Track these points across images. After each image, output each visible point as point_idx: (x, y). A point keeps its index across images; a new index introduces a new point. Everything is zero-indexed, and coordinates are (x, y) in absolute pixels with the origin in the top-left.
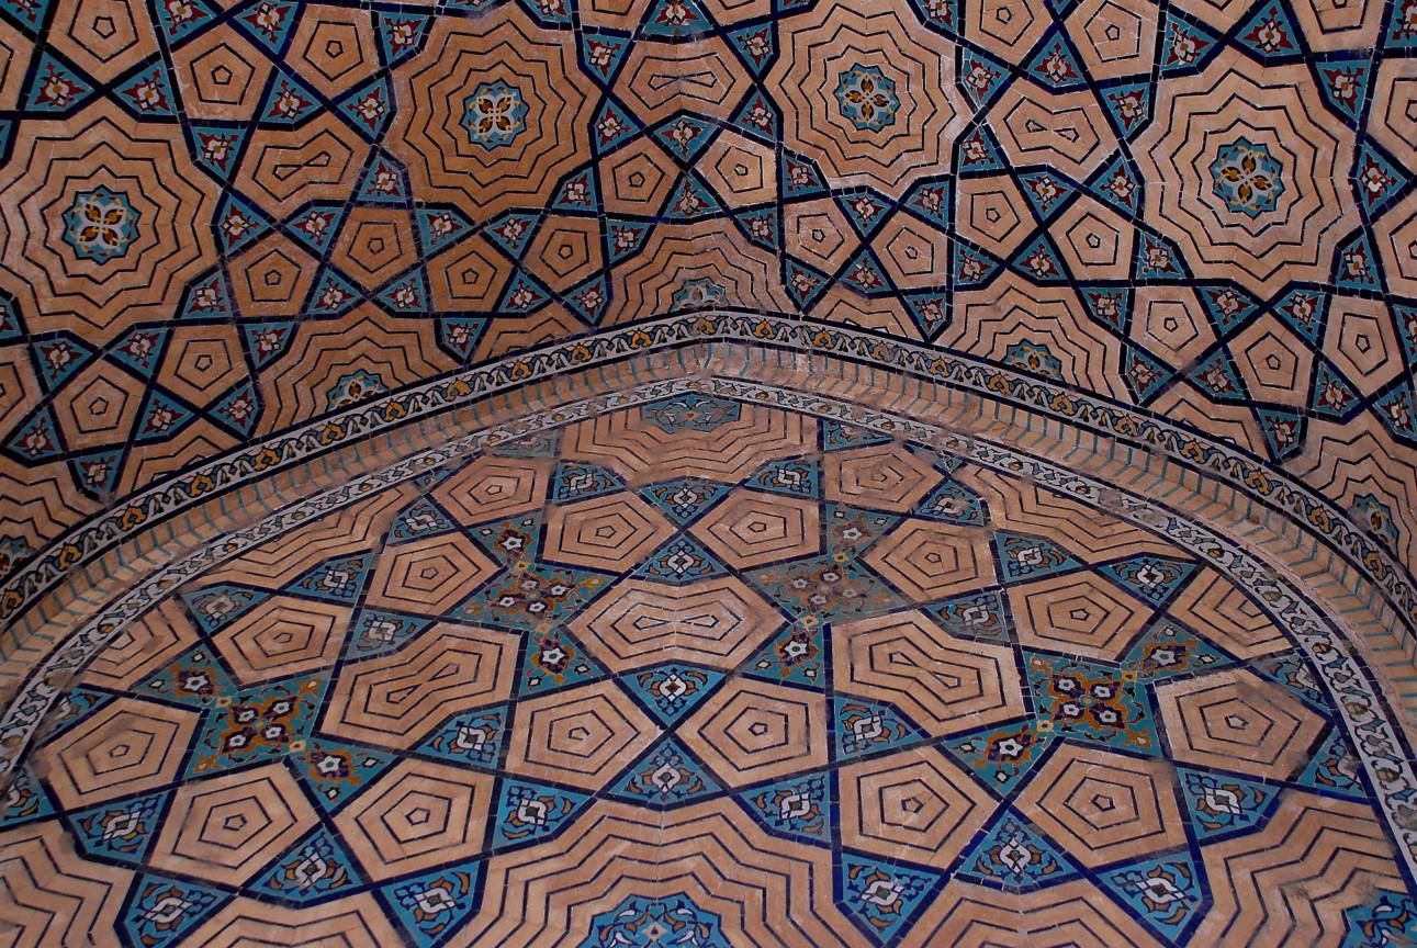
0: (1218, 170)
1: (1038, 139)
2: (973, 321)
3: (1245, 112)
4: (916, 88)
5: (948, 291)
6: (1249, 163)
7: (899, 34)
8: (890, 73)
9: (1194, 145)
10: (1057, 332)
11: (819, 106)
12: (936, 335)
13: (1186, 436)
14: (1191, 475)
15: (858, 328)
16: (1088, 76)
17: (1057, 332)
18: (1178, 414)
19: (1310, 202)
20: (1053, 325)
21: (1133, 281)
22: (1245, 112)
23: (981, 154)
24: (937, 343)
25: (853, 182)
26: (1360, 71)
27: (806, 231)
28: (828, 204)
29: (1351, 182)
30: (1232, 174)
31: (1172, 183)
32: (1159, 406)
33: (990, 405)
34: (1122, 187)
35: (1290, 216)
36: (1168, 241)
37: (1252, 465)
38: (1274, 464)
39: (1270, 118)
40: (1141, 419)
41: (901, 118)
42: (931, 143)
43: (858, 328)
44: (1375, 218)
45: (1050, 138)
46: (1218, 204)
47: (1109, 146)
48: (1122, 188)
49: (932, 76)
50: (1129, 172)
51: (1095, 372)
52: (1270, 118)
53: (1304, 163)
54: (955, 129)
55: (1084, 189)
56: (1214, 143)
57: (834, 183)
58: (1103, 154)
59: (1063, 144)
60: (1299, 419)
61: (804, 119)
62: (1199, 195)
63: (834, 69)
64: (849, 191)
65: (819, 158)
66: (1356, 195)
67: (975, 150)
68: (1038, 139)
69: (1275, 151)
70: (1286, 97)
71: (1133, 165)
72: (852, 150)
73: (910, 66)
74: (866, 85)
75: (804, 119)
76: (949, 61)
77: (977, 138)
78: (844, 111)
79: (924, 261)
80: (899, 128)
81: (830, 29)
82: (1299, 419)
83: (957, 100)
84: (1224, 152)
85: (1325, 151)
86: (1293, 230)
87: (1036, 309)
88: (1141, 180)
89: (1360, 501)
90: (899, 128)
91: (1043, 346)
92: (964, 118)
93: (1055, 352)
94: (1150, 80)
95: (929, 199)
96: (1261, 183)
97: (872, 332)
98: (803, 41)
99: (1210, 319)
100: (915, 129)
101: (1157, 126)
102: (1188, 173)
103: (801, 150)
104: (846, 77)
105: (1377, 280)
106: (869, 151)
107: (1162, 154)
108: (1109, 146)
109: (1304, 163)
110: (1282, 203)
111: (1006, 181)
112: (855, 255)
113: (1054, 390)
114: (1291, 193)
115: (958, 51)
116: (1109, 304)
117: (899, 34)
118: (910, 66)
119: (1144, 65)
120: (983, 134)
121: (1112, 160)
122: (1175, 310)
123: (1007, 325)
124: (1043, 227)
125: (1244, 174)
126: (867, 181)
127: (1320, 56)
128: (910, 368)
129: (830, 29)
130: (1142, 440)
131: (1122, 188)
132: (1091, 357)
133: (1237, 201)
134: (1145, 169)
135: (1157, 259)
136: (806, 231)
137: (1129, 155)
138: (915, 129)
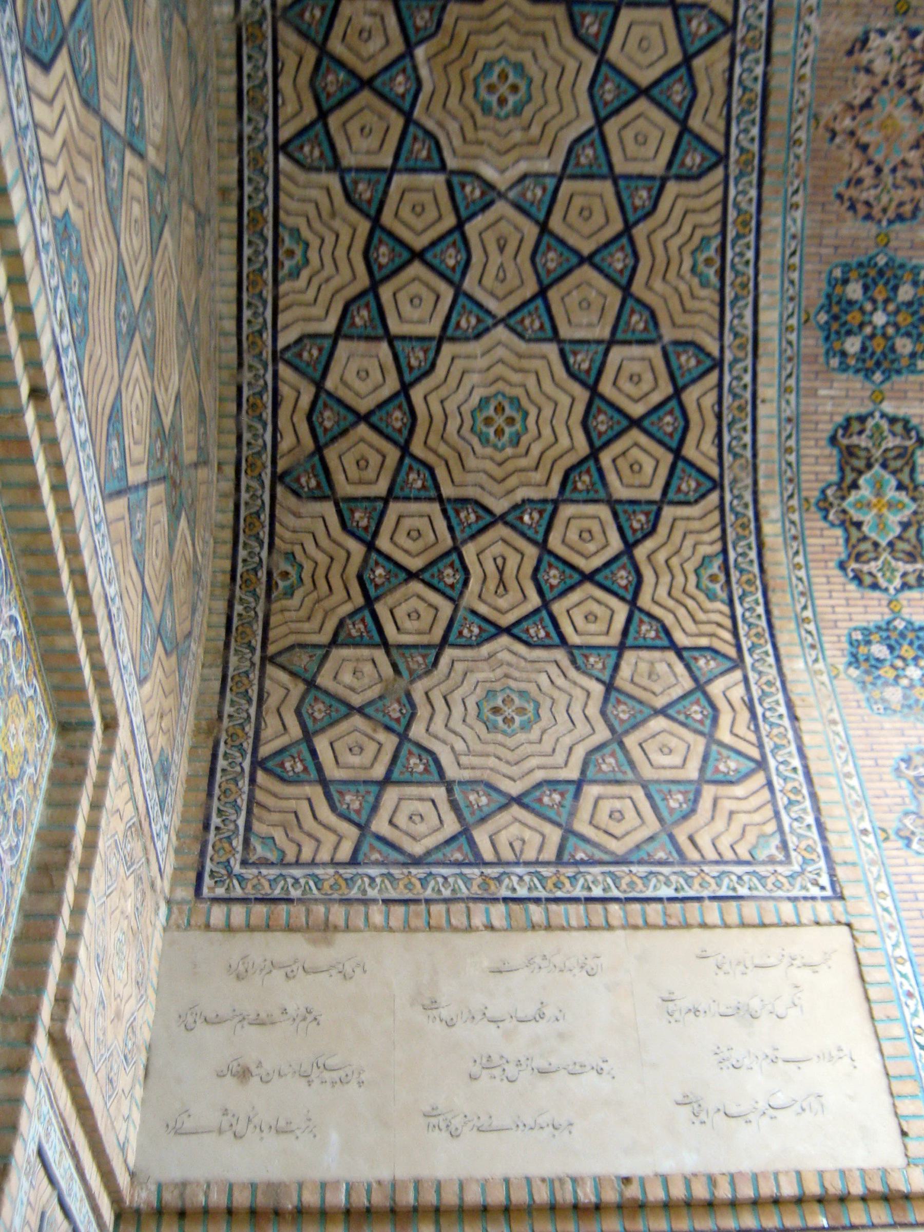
0: (500, 398)
1: (492, 248)
2: (315, 194)
3: (547, 412)
4: (517, 136)
5: (336, 166)
6: (511, 421)
7: (562, 120)
8: (528, 111)
9: (516, 378)
10: (325, 274)
11: (493, 40)
12: (290, 157)
13: (268, 398)
14: (233, 407)
15: (276, 75)
16: (551, 285)
17: (325, 274)
18: (284, 389)
19: (499, 472)
20: (329, 269)
21: (392, 340)
22: (547, 412)
23: (469, 197)
24: (282, 160)
25: (424, 72)
26: (596, 492)
27: (367, 21)
28: (398, 47)
29: (523, 501)
30: (500, 409)
31: (482, 363)
32: (284, 371)
33: (233, 212)
34: (465, 320)
35: (481, 460)
36: (433, 366)
37: (267, 457)
38: (277, 478)
39: (547, 432)
40: (267, 354)
41: (489, 121)
42: (474, 149)
43: (276, 75)
44: (506, 523)
45: (495, 258)
46: (475, 400)
47: (499, 309)
48: (468, 322)
49: (530, 150)
50: (481, 327)
51: (297, 312)
52: (547, 432)
53: (523, 462)
54: (489, 173)
55: (459, 291)
56: (519, 392)
57: (420, 53)
58: (491, 304)
59: (492, 270)
60: (325, 490)
61: (476, 25)
62: (476, 388)
63: (525, 57)
64: (415, 68)
65: (441, 39)
66: (516, 507)
67: (473, 191)
68: (492, 248)
69: (525, 440)
70: (564, 442)
71: (487, 330)
72: (454, 72)
73: (535, 131)
74: (514, 89)
75: (476, 25)
76: (545, 166)
77: (483, 194)
78: (488, 66)
79: (361, 144)
80: (481, 119)
81: (561, 55)
82: (325, 490)
83: (514, 173)
84: (515, 401)
85: (538, 477)
86: (471, 462)
87: (341, 253)
88: (478, 336)
89: (291, 557)
90: (481, 119)
91: (307, 262)
92: (501, 181)
93: (305, 274)
94: (555, 336)
95: (418, 147)
96: (499, 432)
97: (276, 91)
98: (548, 27)
99: (380, 406)
100: (482, 135)
101: (522, 346)
102: (491, 375)
103: (448, 21)
104: (520, 68)
105: (465, 535)
106: (456, 88)
107: (500, 352)
108: (499, 309)
109: (523, 462)
110: (489, 451)
111: (450, 221)
112: (352, 73)
113: (268, 274)
114: (499, 457)
115: (552, 175)
116: (364, 317)
117: (562, 120)
118: (535, 131)
119: (565, 332)
120: (487, 199)
121: (488, 312)
122: (376, 375)
123: (317, 225)
124: (418, 255)
125: (502, 416)
126: (427, 88)
127: (597, 461)
128: (248, 130)
129: (561, 55)
130: (247, 358)
131: (468, 322)
132: (310, 308)
133: (480, 417)
134: (486, 340)
135: (417, 358)
136: (367, 21)
137: (495, 325)
138: (482, 135)
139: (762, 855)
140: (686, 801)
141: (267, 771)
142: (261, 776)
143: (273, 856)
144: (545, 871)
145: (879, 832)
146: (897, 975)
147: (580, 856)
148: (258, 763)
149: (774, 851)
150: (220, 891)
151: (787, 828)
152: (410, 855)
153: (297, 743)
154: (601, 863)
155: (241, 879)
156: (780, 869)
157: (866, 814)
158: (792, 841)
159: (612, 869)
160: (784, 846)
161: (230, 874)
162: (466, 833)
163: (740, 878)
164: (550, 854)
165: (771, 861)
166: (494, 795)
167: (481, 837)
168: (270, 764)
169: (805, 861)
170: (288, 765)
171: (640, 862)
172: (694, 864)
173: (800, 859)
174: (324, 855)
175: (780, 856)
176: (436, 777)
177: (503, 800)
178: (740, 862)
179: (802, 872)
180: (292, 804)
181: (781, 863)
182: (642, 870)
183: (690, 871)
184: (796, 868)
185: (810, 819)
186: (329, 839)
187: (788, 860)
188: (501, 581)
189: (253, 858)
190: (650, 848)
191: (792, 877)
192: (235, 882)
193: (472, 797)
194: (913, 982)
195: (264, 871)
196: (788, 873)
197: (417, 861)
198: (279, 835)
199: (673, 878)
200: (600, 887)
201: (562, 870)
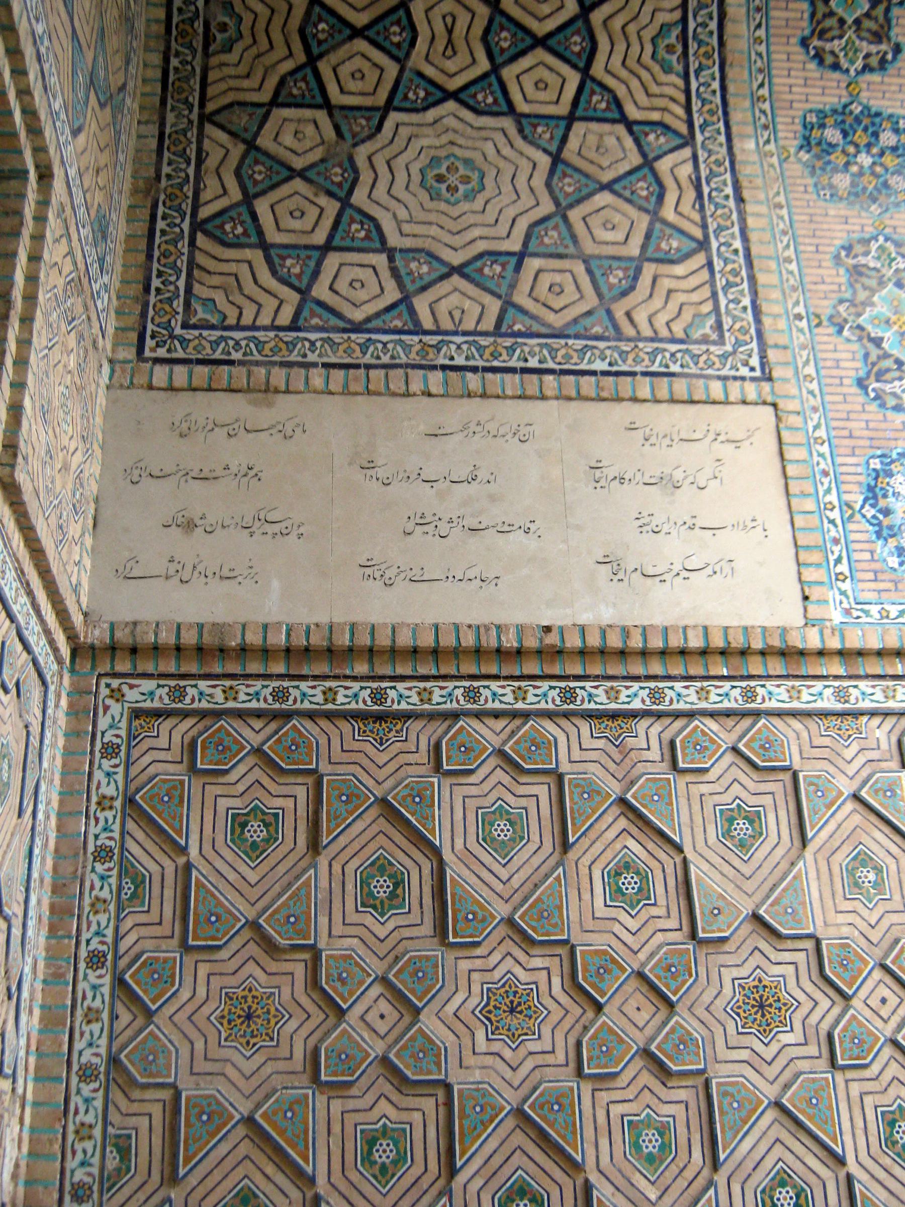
139: (697, 335)
141: (206, 233)
142: (201, 239)
143: (214, 320)
144: (484, 341)
145: (845, 508)
146: (825, 521)
147: (516, 327)
148: (197, 226)
149: (707, 330)
150: (162, 352)
151: (723, 310)
152: (350, 321)
153: (237, 205)
154: (539, 335)
155: (183, 341)
156: (712, 348)
157: (844, 554)
158: (727, 322)
159: (549, 341)
160: (719, 326)
161: (172, 337)
162: (406, 300)
163: (673, 355)
164: (488, 324)
165: (705, 340)
166: (435, 264)
167: (421, 305)
168: (209, 226)
169: (738, 343)
170: (228, 227)
171: (577, 336)
172: (629, 340)
175: (714, 337)
176: (378, 245)
177: (445, 270)
178: (674, 340)
179: (734, 352)
180: (232, 267)
181: (714, 343)
182: (579, 344)
184: (728, 348)
185: (746, 301)
186: (270, 304)
187: (721, 341)
188: (450, 41)
189: (193, 321)
190: (587, 322)
191: (724, 357)
194: (840, 528)
195: (205, 333)
197: (357, 328)
198: (219, 297)
200: (537, 358)
201: (499, 340)
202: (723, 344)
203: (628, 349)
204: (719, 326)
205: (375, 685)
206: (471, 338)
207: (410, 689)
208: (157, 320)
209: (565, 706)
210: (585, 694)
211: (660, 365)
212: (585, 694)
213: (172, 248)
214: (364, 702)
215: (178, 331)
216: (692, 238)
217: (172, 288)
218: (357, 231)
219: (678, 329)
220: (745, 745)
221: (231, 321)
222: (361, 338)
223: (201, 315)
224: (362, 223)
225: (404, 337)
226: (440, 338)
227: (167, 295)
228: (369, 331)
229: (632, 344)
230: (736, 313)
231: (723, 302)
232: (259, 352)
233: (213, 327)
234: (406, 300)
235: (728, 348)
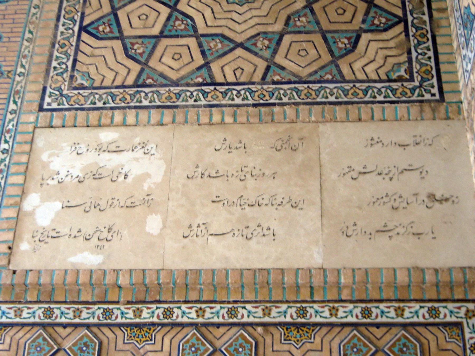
139: (394, 76)
140: (349, 43)
142: (85, 36)
143: (86, 84)
144: (253, 87)
147: (277, 78)
148: (83, 29)
149: (402, 73)
150: (54, 106)
151: (414, 59)
153: (108, 15)
154: (289, 82)
155: (68, 97)
158: (416, 67)
159: (297, 85)
161: (61, 95)
162: (207, 65)
163: (379, 90)
164: (257, 77)
165: (400, 79)
166: (226, 42)
167: (215, 67)
168: (89, 29)
169: (423, 80)
170: (101, 28)
171: (314, 82)
172: (348, 82)
173: (419, 78)
174: (118, 82)
176: (192, 33)
177: (232, 46)
178: (381, 81)
179: (421, 86)
180: (103, 52)
181: (407, 80)
182: (316, 86)
183: (347, 86)
184: (417, 84)
185: (431, 54)
186: (123, 72)
187: (412, 79)
189: (75, 84)
190: (321, 73)
191: (413, 90)
192: (64, 99)
193: (212, 45)
195: (81, 92)
196: (411, 87)
197: (176, 84)
198: (92, 70)
199: (335, 91)
200: (287, 98)
201: (265, 87)
202: (413, 81)
203: (348, 88)
204: (410, 71)
205: (105, 306)
206: (246, 87)
207: (69, 309)
208: (53, 86)
209: (105, 321)
210: (119, 312)
211: (371, 97)
212: (119, 312)
213: (67, 43)
214: (39, 317)
215: (65, 92)
216: (395, 16)
217: (64, 66)
218: (180, 25)
219: (382, 73)
220: (226, 349)
221: (97, 84)
222: (176, 90)
223: (79, 81)
224: (182, 21)
225: (203, 88)
226: (227, 87)
227: (61, 70)
228: (182, 85)
229: (351, 85)
230: (423, 61)
231: (414, 54)
232: (113, 101)
233: (85, 88)
234: (207, 65)
235: (417, 84)
